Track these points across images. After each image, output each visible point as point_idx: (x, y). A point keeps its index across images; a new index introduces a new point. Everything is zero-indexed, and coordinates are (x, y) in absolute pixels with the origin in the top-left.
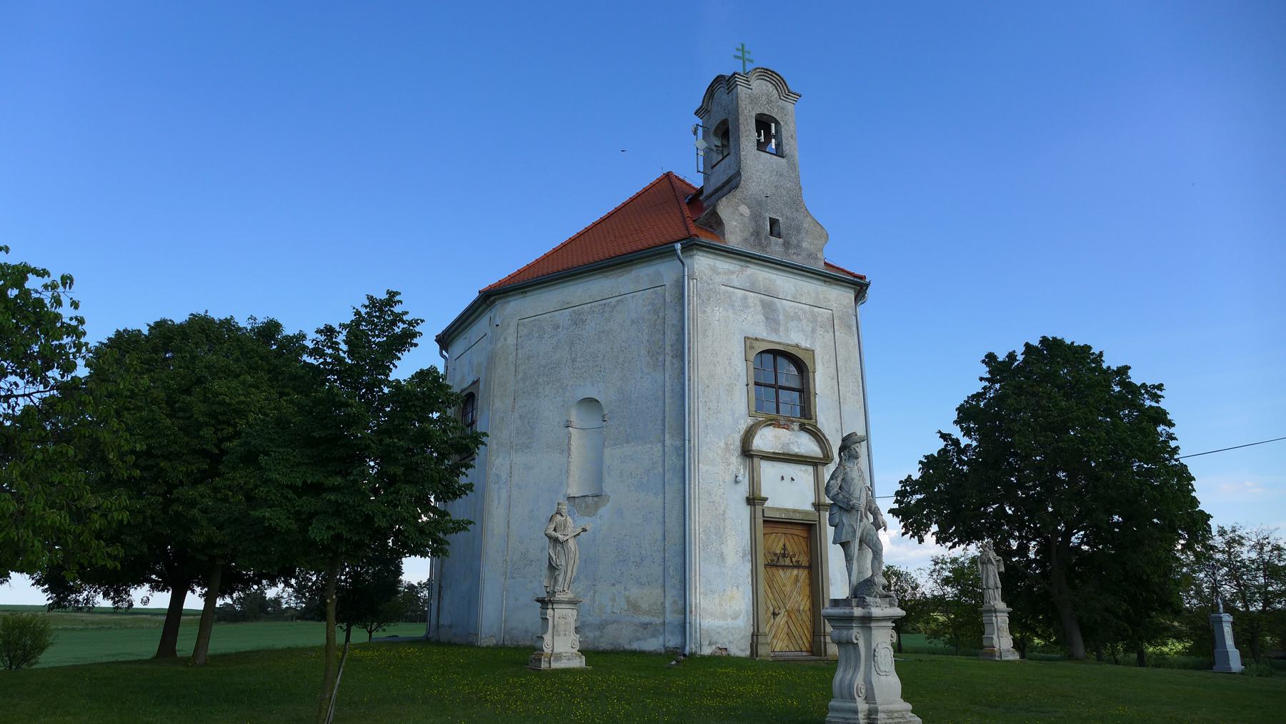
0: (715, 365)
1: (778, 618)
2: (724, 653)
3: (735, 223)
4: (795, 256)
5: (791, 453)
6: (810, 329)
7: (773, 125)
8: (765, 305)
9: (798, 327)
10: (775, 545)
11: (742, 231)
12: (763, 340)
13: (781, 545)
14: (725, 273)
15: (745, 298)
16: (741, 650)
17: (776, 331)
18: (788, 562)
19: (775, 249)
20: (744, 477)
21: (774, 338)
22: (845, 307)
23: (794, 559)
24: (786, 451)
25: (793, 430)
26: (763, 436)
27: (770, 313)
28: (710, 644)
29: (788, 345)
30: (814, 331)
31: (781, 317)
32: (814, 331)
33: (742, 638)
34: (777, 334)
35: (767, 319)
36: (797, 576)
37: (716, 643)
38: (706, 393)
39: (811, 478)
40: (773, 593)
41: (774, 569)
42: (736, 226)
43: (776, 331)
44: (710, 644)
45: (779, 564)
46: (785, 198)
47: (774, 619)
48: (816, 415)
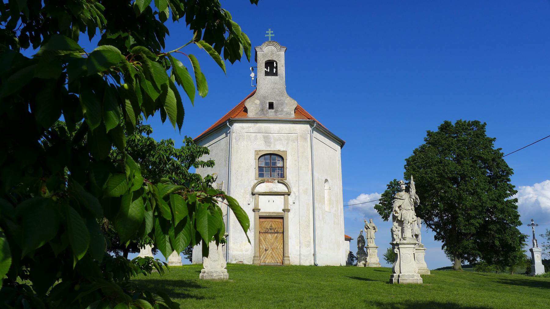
0: (241, 163)
1: (267, 251)
2: (241, 263)
3: (252, 108)
4: (280, 115)
5: (273, 191)
6: (286, 143)
7: (275, 63)
8: (264, 137)
9: (280, 143)
10: (267, 225)
11: (255, 110)
12: (263, 151)
13: (270, 225)
14: (247, 128)
15: (256, 136)
16: (249, 262)
17: (270, 146)
18: (273, 231)
19: (271, 114)
20: (252, 202)
21: (268, 149)
22: (304, 131)
23: (275, 230)
24: (271, 191)
25: (275, 183)
26: (261, 187)
27: (267, 140)
28: (235, 260)
29: (274, 151)
30: (288, 143)
31: (272, 140)
32: (288, 143)
33: (249, 258)
34: (270, 147)
35: (265, 142)
36: (277, 236)
37: (238, 260)
38: (237, 174)
39: (283, 200)
40: (265, 243)
41: (266, 234)
42: (253, 109)
43: (270, 146)
44: (235, 260)
45: (268, 232)
46: (277, 92)
47: (266, 251)
48: (286, 176)
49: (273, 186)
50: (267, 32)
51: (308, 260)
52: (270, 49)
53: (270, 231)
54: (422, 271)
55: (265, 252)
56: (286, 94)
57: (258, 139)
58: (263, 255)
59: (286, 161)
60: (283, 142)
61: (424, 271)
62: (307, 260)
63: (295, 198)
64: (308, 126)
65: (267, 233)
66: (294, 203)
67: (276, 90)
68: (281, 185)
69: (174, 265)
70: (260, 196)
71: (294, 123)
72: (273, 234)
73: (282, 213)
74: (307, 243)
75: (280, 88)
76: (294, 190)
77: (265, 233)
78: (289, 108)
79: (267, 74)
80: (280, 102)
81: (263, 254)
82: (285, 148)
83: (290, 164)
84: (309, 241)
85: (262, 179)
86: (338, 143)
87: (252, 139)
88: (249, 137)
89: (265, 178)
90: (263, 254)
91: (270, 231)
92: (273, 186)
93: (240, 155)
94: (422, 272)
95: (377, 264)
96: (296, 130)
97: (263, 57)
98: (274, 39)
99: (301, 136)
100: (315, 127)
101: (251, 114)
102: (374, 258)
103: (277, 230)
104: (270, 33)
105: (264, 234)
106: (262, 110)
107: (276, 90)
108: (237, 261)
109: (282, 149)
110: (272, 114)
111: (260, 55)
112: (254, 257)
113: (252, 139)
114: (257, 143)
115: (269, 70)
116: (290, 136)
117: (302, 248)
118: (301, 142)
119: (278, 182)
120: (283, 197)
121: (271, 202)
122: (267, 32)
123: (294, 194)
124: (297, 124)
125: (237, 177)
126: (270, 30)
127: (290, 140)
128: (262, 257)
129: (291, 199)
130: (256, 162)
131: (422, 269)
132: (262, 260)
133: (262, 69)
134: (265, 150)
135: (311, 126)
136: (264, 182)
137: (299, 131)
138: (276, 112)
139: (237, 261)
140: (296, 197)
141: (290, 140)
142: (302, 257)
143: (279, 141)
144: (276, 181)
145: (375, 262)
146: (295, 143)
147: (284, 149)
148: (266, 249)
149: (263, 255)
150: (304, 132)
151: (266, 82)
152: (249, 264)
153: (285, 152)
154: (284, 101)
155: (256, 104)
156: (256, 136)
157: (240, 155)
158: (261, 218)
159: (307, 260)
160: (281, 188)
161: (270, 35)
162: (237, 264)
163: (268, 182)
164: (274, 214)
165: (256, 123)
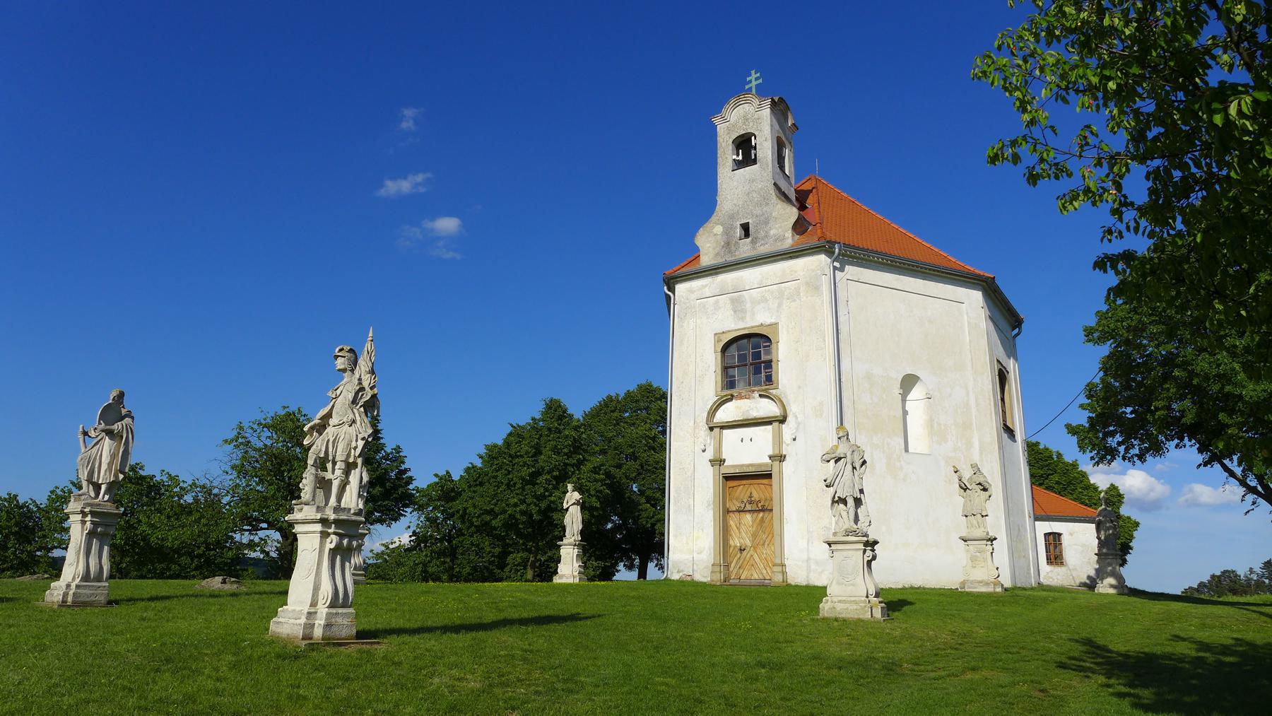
0: (688, 365)
1: (745, 553)
2: (689, 579)
3: (708, 245)
4: (762, 247)
5: (750, 418)
6: (777, 305)
7: (753, 138)
8: (733, 301)
9: (764, 308)
10: (742, 494)
11: (714, 249)
12: (729, 331)
13: (748, 494)
14: (699, 290)
15: (717, 302)
16: (704, 577)
17: (743, 319)
18: (755, 507)
19: (745, 249)
20: (710, 445)
21: (741, 325)
22: (813, 271)
23: (760, 505)
24: (745, 418)
25: (754, 398)
26: (726, 410)
27: (738, 307)
28: (678, 572)
29: (752, 327)
30: (780, 305)
31: (748, 305)
32: (780, 305)
33: (705, 568)
34: (743, 321)
35: (735, 312)
36: (763, 518)
37: (683, 571)
38: (681, 389)
39: (770, 436)
40: (740, 533)
41: (742, 514)
42: (710, 247)
43: (743, 319)
44: (678, 572)
45: (746, 509)
46: (756, 199)
47: (741, 553)
48: (778, 380)
49: (750, 407)
50: (748, 79)
51: (826, 573)
52: (742, 111)
53: (749, 507)
54: (847, 605)
55: (739, 554)
56: (774, 197)
57: (720, 308)
58: (735, 561)
59: (777, 345)
60: (771, 304)
61: (855, 607)
62: (822, 572)
63: (797, 429)
64: (823, 258)
65: (743, 511)
66: (794, 439)
67: (755, 195)
68: (766, 400)
69: (563, 582)
70: (725, 432)
71: (791, 258)
72: (756, 514)
73: (766, 465)
74: (824, 533)
75: (761, 189)
76: (793, 410)
77: (739, 511)
78: (781, 227)
79: (739, 165)
80: (762, 218)
81: (736, 558)
82: (774, 317)
83: (784, 354)
84: (828, 526)
85: (729, 392)
86: (974, 283)
87: (708, 310)
88: (704, 307)
89: (734, 392)
90: (736, 558)
91: (749, 507)
92: (750, 407)
93: (687, 347)
94: (847, 609)
95: (987, 584)
96: (795, 272)
97: (728, 133)
98: (761, 92)
99: (807, 284)
100: (839, 254)
101: (706, 260)
102: (982, 567)
103: (762, 503)
104: (754, 79)
105: (737, 514)
106: (728, 244)
107: (755, 195)
108: (681, 574)
109: (768, 321)
110: (746, 248)
111: (722, 130)
112: (712, 565)
113: (708, 310)
114: (720, 317)
115: (740, 158)
116: (783, 289)
117: (812, 543)
118: (807, 297)
119: (760, 396)
120: (770, 427)
121: (747, 440)
122: (748, 79)
123: (794, 419)
124: (797, 257)
125: (680, 395)
126: (753, 72)
127: (785, 297)
128: (733, 565)
129: (787, 429)
130: (716, 358)
131: (851, 602)
132: (734, 573)
133: (727, 154)
134: (734, 329)
135: (829, 253)
136: (731, 400)
137: (802, 274)
138: (753, 242)
139: (681, 574)
140: (799, 424)
141: (785, 297)
142: (813, 567)
143: (762, 304)
144: (756, 395)
145: (985, 578)
146: (794, 300)
147: (773, 321)
148: (741, 547)
149: (735, 561)
150: (813, 274)
151: (735, 183)
152: (704, 580)
153: (774, 326)
154: (771, 214)
155: (715, 235)
156: (717, 302)
157: (687, 347)
158: (727, 478)
159: (822, 572)
160: (766, 408)
161: (754, 83)
162: (683, 582)
163: (740, 397)
164: (751, 469)
165: (716, 274)
